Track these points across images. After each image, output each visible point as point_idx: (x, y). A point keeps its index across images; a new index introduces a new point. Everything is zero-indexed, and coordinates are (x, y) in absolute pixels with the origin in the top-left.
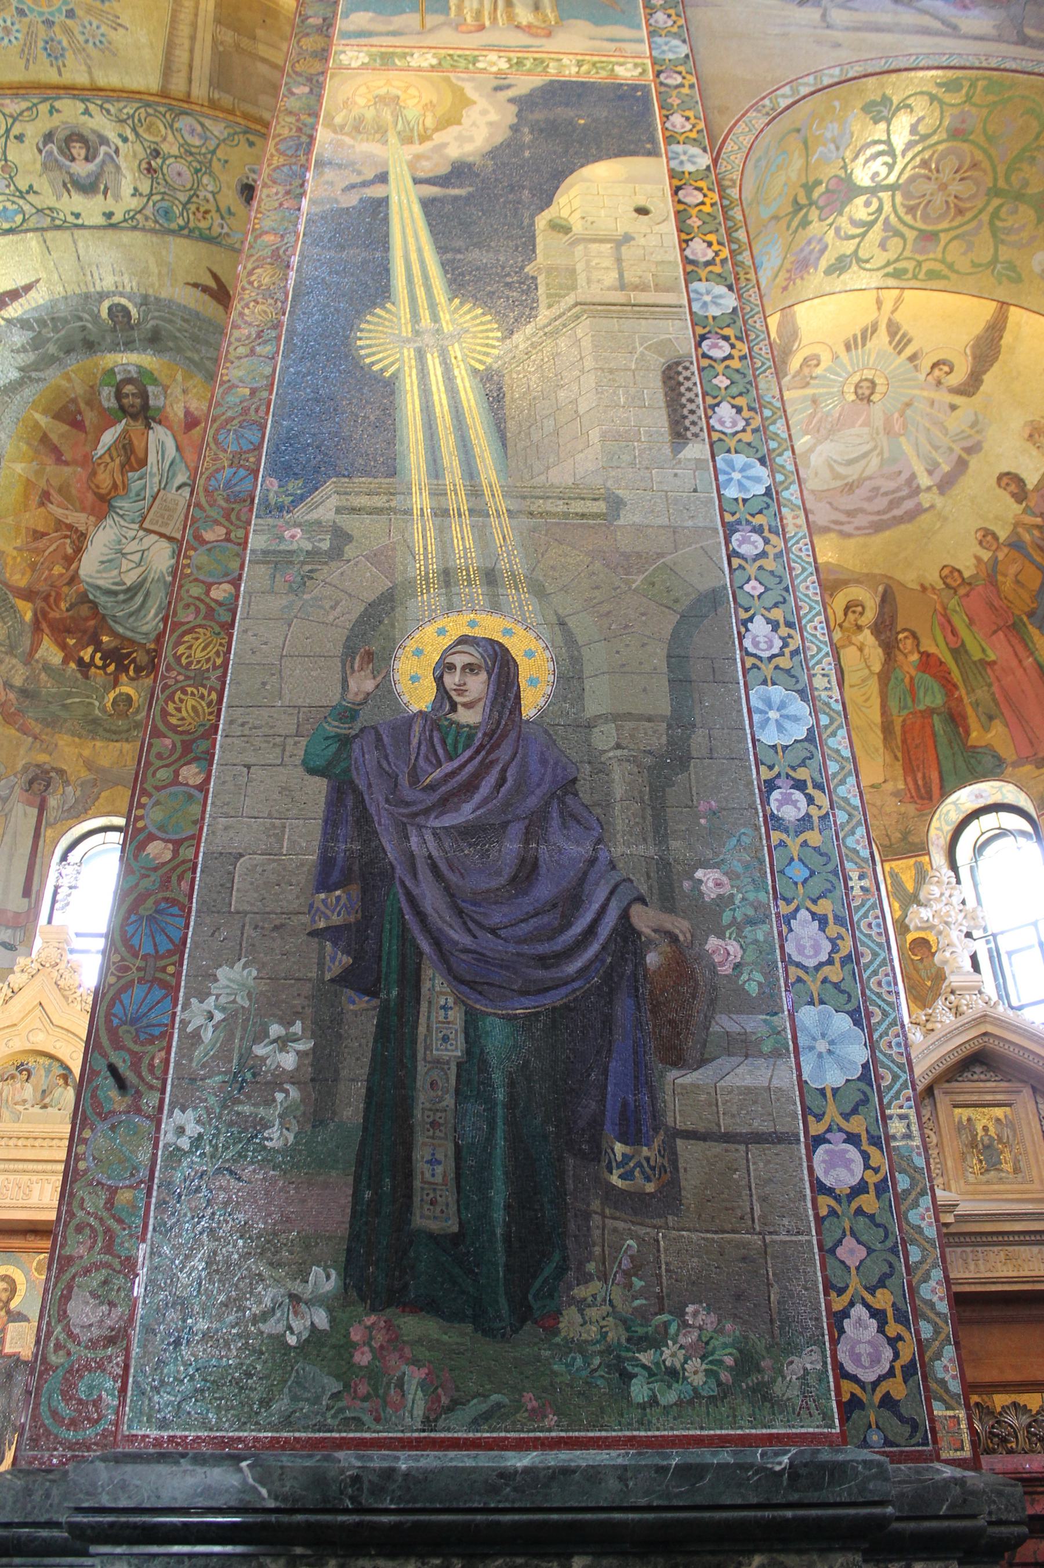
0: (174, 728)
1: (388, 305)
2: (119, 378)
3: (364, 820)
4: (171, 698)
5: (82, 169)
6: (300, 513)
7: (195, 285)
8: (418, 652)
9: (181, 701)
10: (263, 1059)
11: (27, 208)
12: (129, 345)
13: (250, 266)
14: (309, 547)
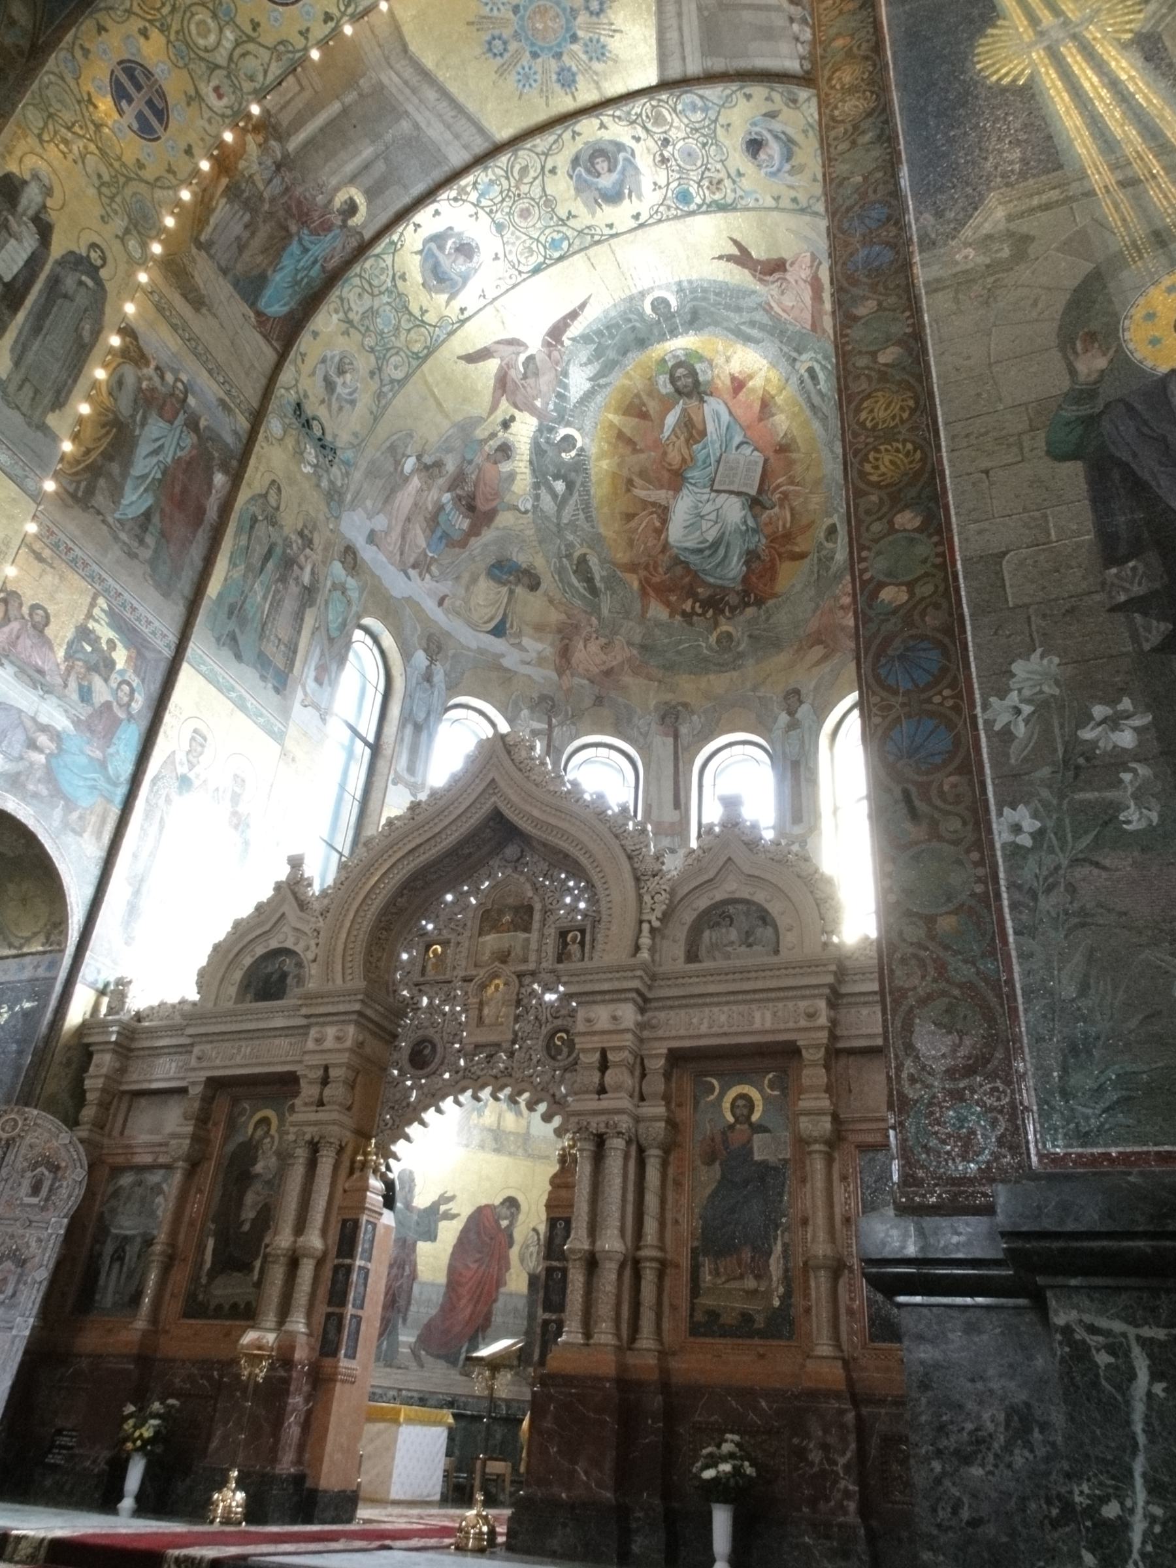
0: (877, 485)
1: (999, 23)
2: (670, 364)
3: (1138, 488)
4: (865, 459)
5: (607, 181)
6: (967, 233)
7: (720, 258)
8: (1150, 316)
9: (877, 459)
10: (1094, 744)
11: (570, 233)
12: (674, 333)
13: (827, 74)
14: (988, 261)
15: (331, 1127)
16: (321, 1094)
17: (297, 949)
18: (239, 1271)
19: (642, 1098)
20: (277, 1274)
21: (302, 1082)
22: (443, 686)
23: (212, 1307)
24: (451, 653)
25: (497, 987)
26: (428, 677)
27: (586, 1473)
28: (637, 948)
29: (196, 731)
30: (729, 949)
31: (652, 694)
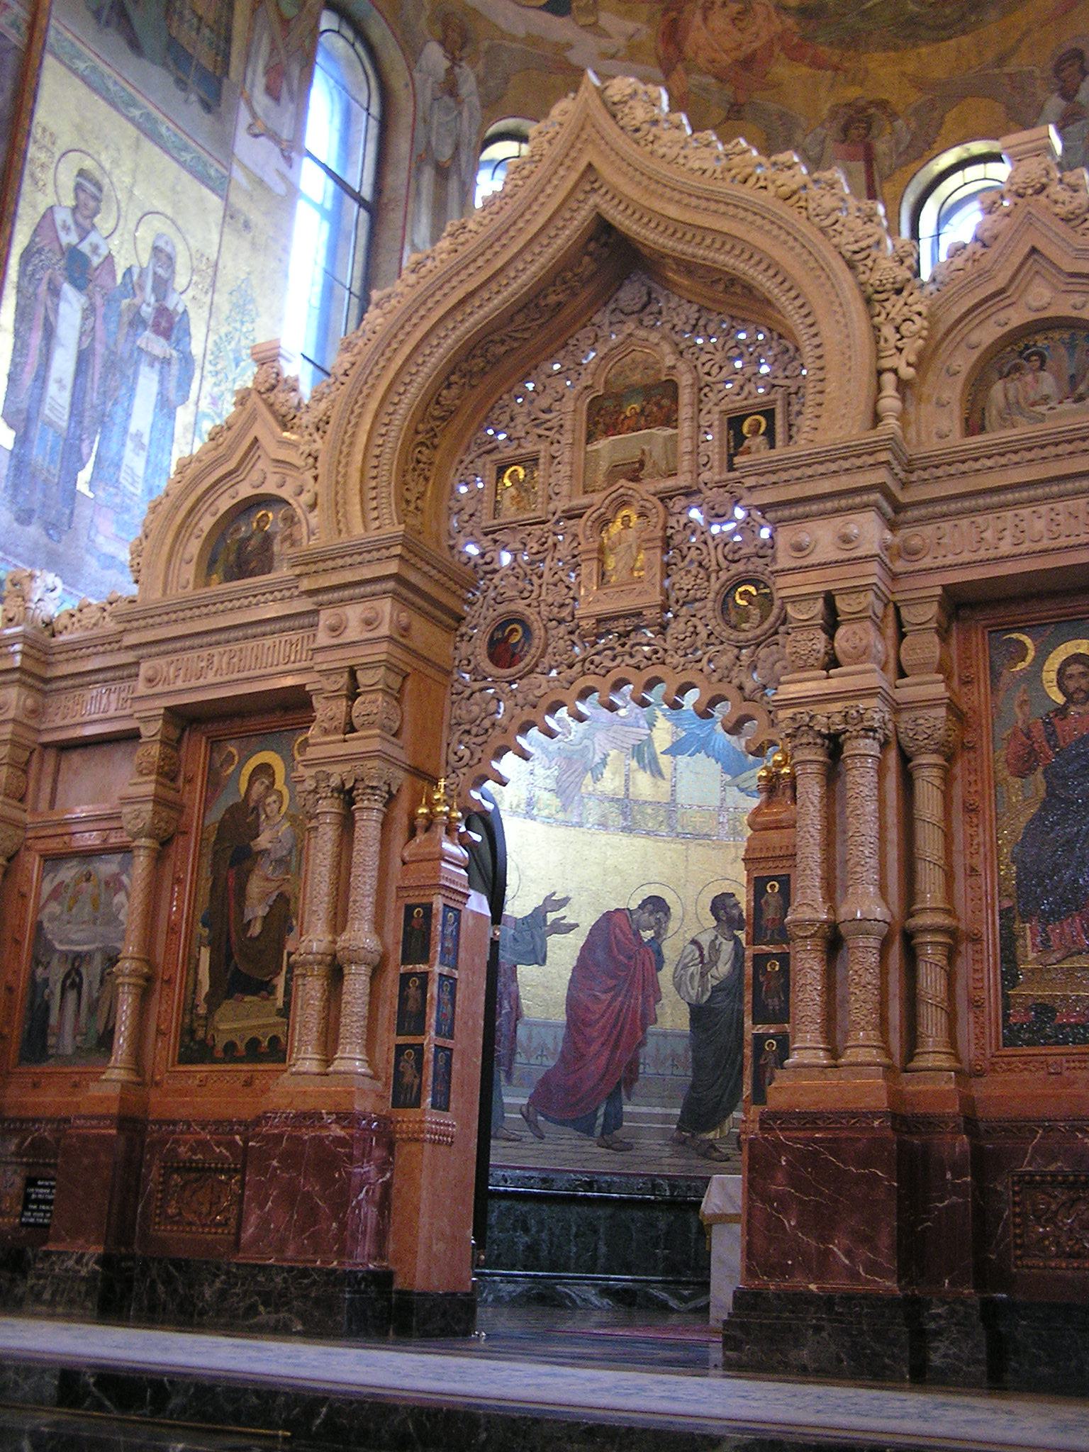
15: (369, 764)
16: (349, 714)
17: (285, 493)
18: (254, 994)
19: (902, 674)
20: (312, 990)
21: (317, 702)
22: (475, 101)
23: (220, 1046)
24: (485, 45)
25: (626, 522)
26: (451, 88)
27: (848, 1254)
28: (877, 418)
29: (82, 173)
30: (1042, 409)
31: (823, 93)
